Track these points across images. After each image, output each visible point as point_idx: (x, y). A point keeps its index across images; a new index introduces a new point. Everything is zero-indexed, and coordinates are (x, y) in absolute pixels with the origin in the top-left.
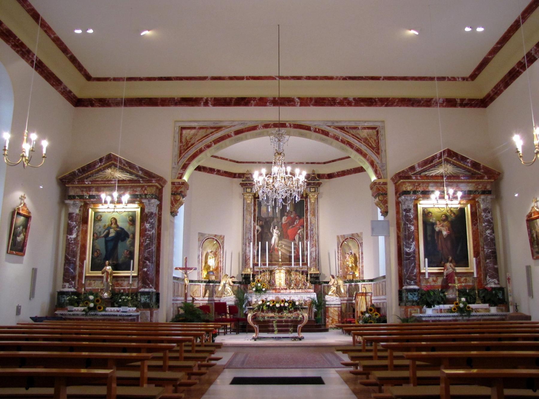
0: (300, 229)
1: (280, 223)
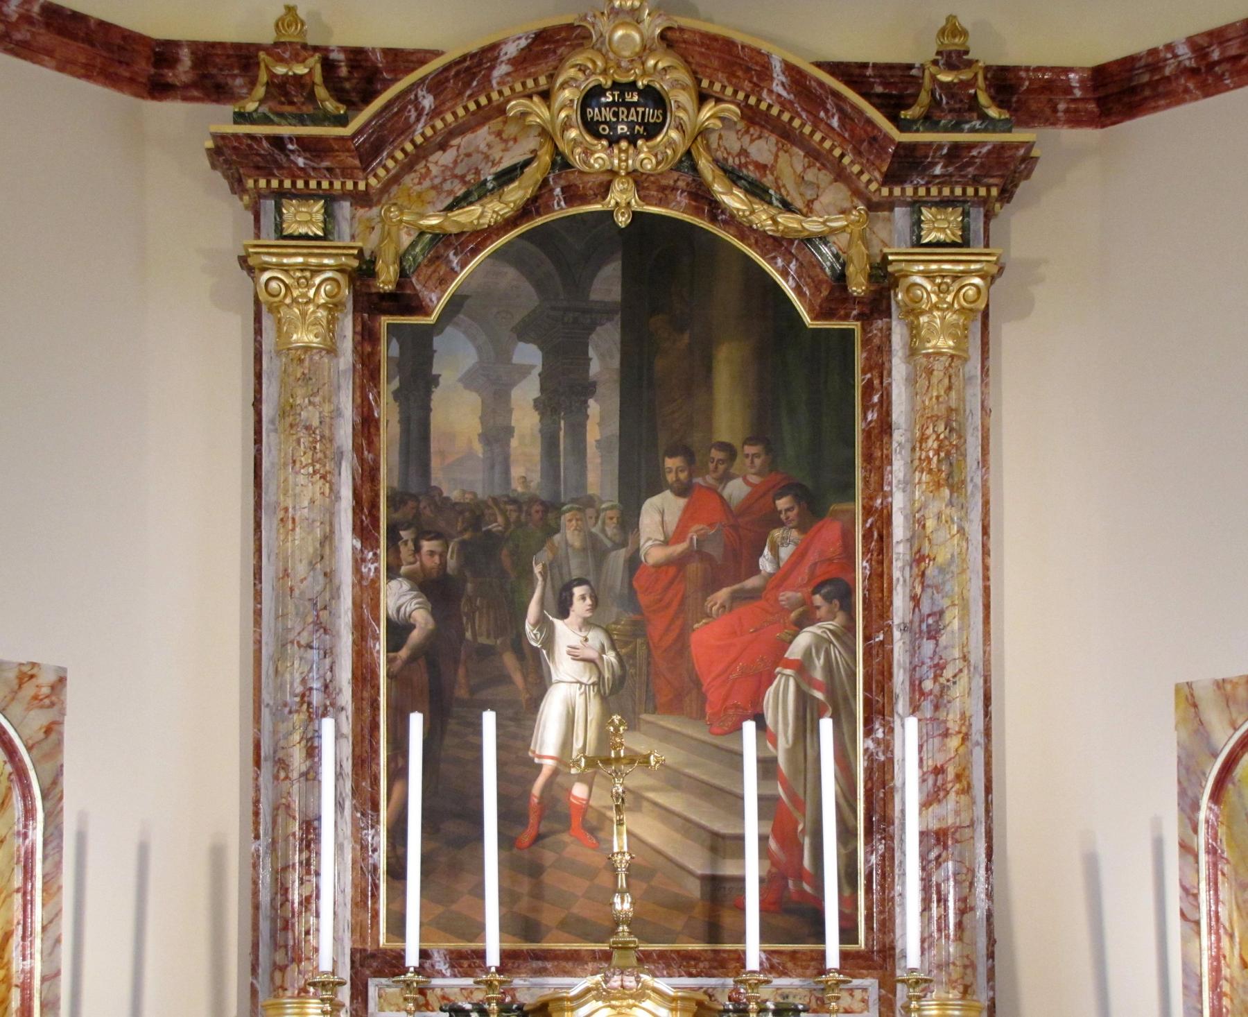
1: (621, 555)
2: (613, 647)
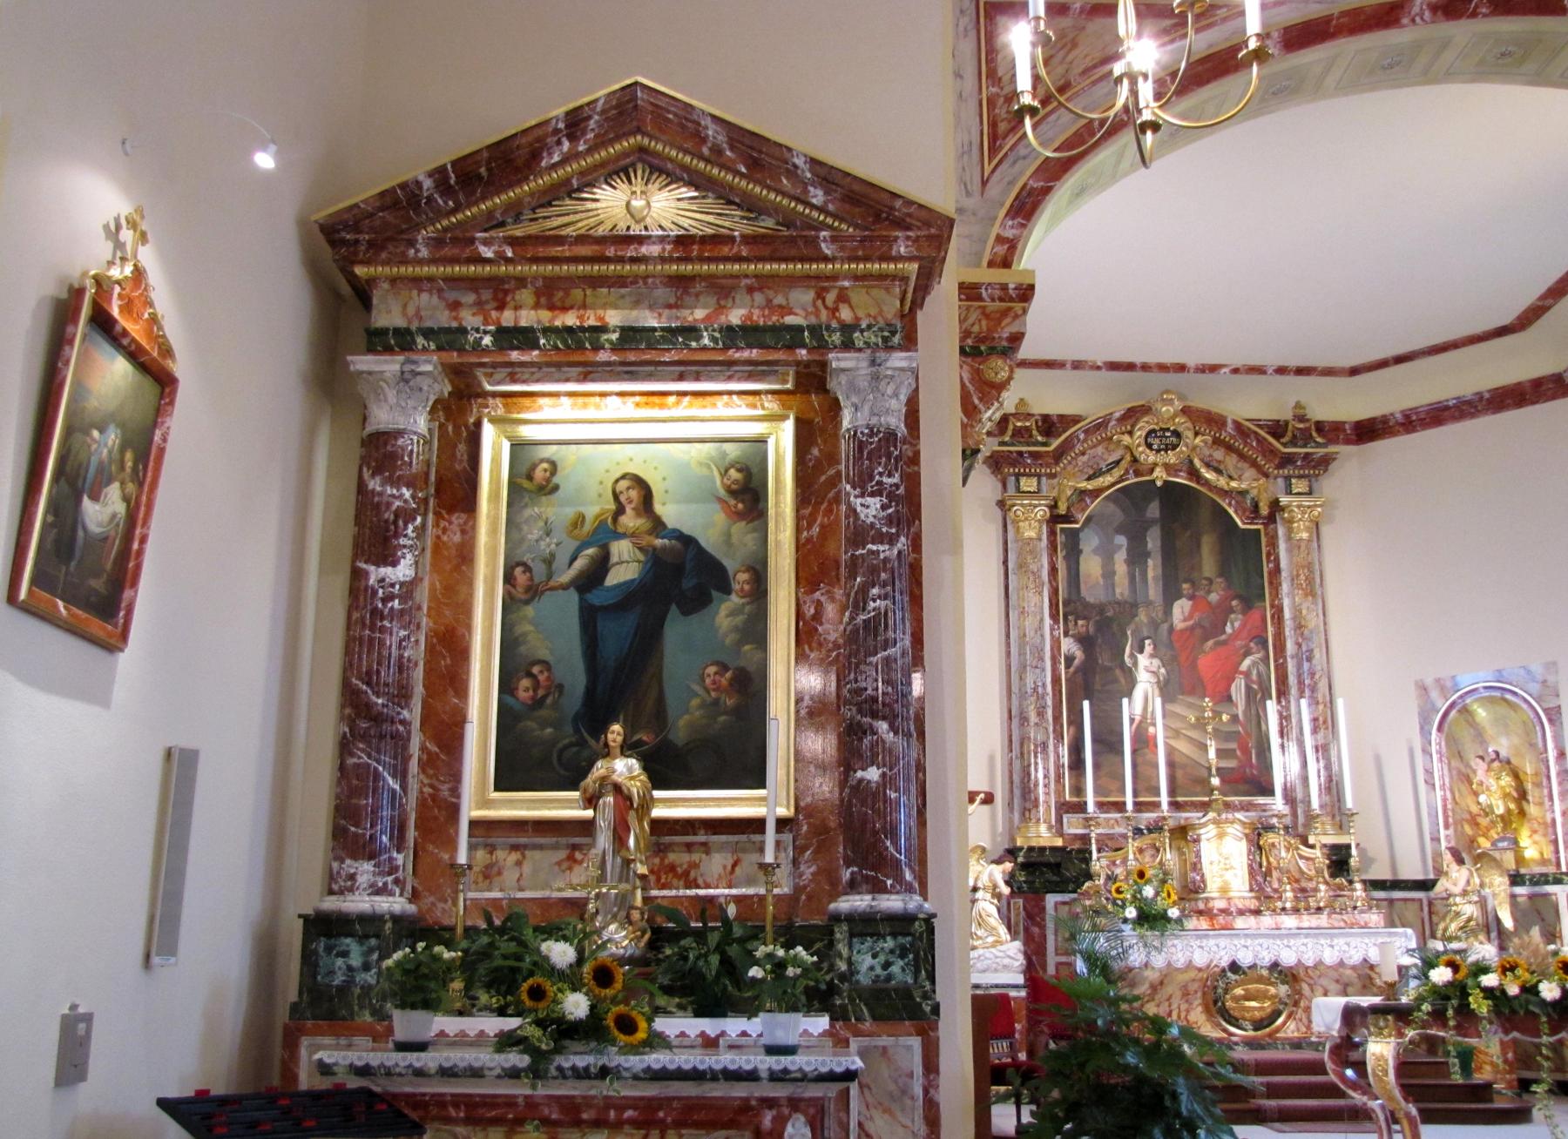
0: (1247, 653)
1: (1165, 626)
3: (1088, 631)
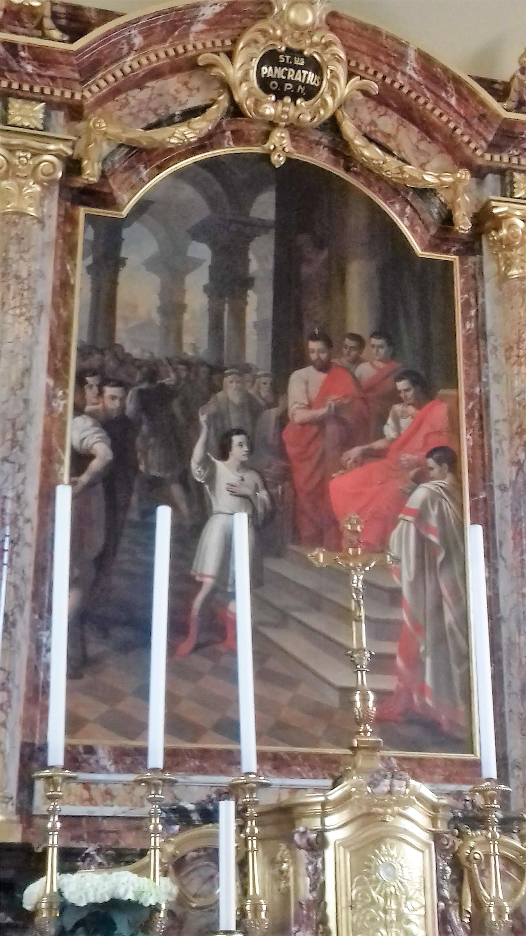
1: (273, 413)
2: (266, 486)
3: (123, 408)
